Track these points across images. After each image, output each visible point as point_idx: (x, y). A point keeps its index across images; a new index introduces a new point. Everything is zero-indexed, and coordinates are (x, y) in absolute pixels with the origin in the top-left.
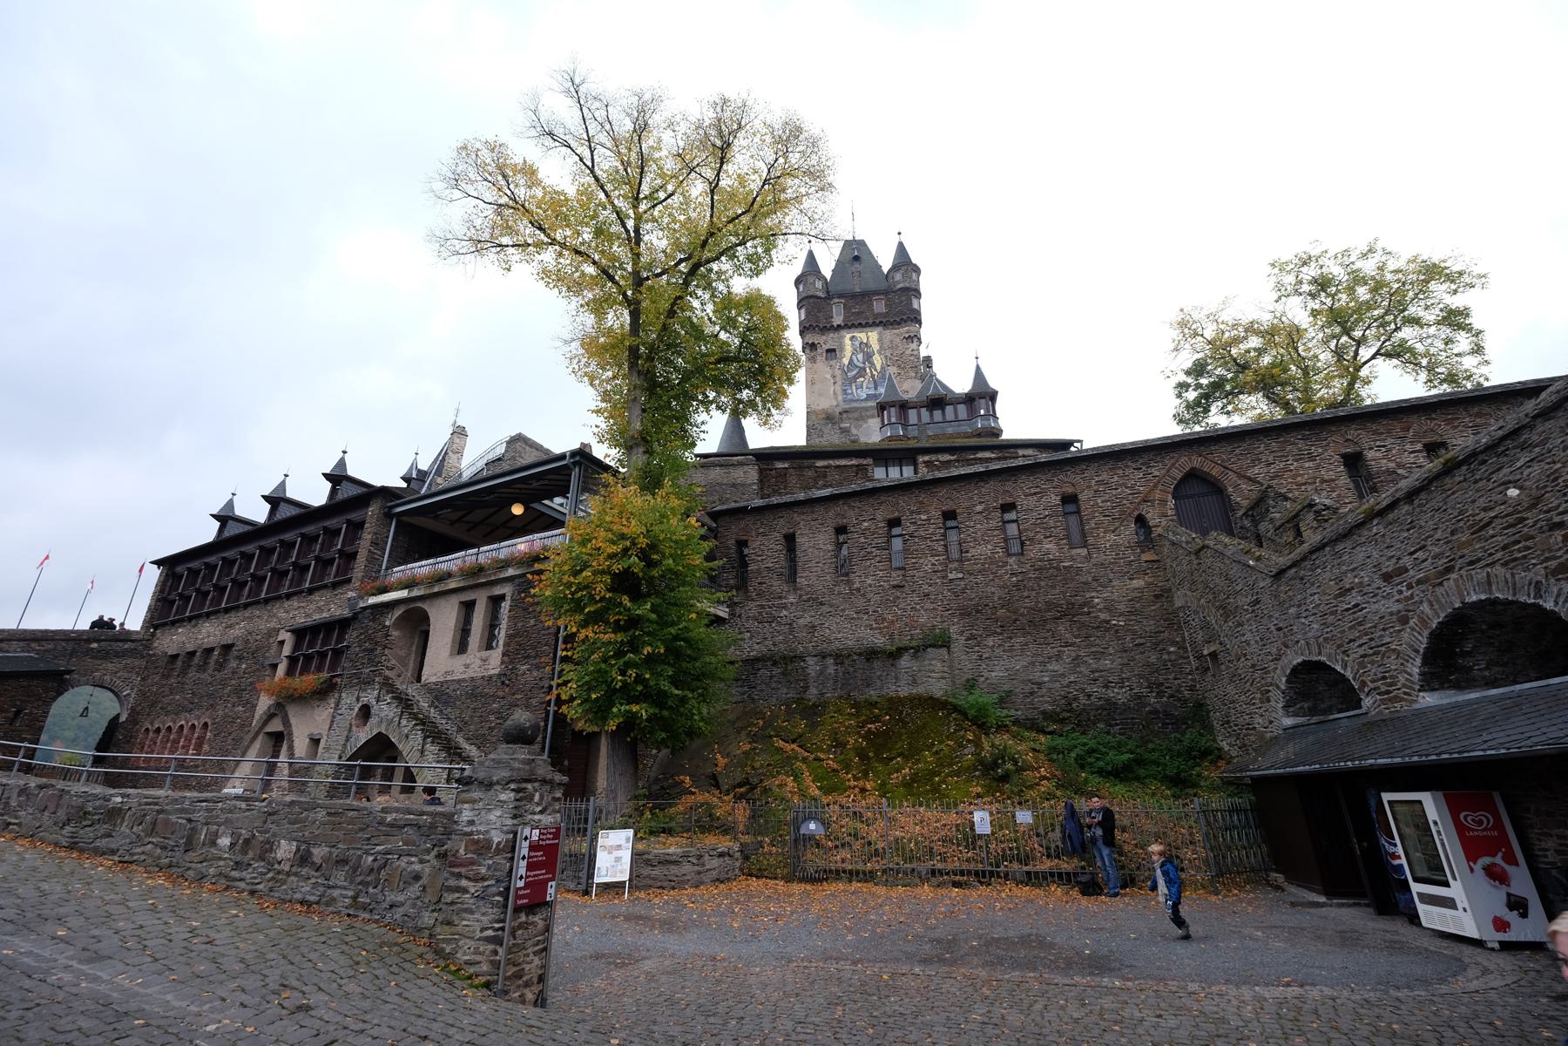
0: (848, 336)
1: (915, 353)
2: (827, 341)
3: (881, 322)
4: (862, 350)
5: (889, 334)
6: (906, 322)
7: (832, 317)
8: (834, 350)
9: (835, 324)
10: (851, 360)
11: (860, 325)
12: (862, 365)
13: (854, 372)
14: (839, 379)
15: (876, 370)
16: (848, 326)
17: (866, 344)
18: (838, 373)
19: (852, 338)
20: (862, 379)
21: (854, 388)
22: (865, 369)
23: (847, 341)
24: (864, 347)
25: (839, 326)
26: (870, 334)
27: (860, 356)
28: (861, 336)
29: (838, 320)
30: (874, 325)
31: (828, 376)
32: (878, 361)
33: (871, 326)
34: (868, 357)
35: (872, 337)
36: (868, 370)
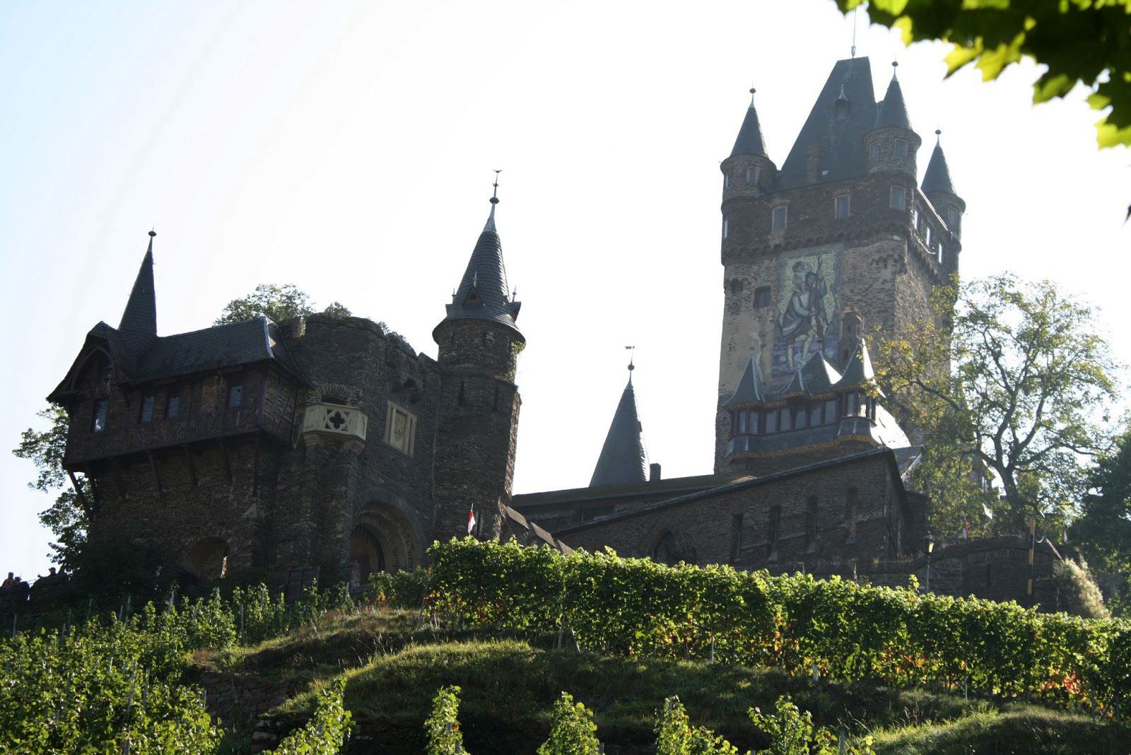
0: (791, 263)
1: (888, 286)
2: (760, 274)
3: (841, 235)
4: (809, 288)
5: (851, 256)
6: (878, 232)
7: (768, 232)
8: (768, 289)
9: (772, 244)
10: (791, 303)
11: (809, 243)
12: (805, 313)
13: (793, 326)
14: (770, 338)
15: (825, 319)
16: (792, 245)
17: (816, 275)
18: (770, 327)
19: (797, 267)
20: (803, 337)
21: (790, 351)
22: (808, 319)
23: (789, 273)
24: (814, 285)
25: (777, 246)
26: (824, 257)
27: (805, 298)
28: (810, 262)
29: (776, 238)
30: (830, 241)
31: (755, 336)
32: (829, 303)
33: (827, 242)
34: (817, 297)
35: (825, 262)
36: (814, 322)
